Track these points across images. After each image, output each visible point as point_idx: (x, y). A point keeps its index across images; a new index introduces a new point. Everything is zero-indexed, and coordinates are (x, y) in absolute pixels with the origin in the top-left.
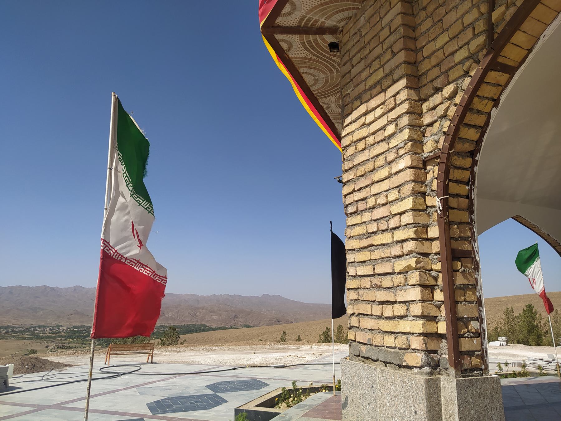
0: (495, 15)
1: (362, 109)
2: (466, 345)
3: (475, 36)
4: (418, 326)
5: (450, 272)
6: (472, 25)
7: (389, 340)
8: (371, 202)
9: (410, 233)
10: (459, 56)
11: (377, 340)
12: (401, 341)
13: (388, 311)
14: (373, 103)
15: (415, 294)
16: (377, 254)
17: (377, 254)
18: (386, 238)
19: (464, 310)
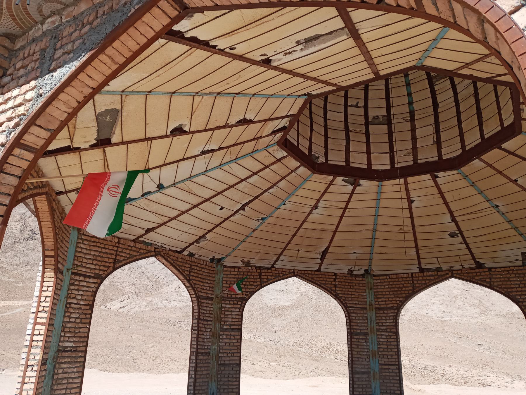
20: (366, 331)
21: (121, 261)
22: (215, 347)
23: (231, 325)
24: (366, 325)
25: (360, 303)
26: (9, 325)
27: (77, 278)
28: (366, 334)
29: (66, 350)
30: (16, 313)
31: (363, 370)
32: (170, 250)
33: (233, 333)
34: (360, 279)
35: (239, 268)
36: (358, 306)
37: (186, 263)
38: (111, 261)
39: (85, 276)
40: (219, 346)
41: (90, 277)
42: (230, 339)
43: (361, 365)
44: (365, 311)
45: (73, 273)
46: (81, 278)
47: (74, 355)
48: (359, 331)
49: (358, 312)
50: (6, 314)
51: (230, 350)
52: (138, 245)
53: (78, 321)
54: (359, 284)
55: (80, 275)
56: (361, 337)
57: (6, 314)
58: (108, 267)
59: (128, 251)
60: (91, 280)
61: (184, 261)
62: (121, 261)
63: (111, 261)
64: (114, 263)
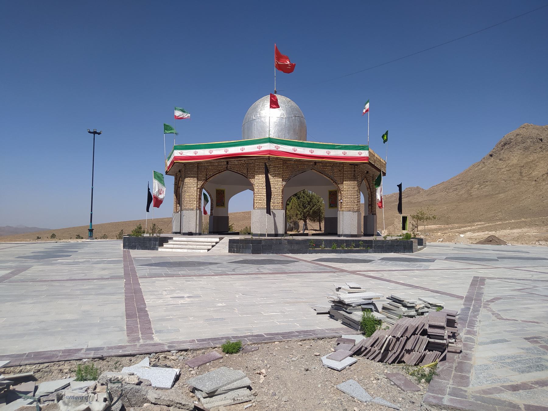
1: (190, 179)
2: (200, 208)
4: (196, 206)
5: (199, 201)
7: (192, 208)
8: (190, 191)
9: (196, 196)
10: (203, 178)
11: (190, 208)
12: (193, 208)
13: (192, 204)
14: (191, 179)
15: (196, 203)
16: (190, 198)
17: (190, 198)
18: (192, 196)
19: (200, 204)
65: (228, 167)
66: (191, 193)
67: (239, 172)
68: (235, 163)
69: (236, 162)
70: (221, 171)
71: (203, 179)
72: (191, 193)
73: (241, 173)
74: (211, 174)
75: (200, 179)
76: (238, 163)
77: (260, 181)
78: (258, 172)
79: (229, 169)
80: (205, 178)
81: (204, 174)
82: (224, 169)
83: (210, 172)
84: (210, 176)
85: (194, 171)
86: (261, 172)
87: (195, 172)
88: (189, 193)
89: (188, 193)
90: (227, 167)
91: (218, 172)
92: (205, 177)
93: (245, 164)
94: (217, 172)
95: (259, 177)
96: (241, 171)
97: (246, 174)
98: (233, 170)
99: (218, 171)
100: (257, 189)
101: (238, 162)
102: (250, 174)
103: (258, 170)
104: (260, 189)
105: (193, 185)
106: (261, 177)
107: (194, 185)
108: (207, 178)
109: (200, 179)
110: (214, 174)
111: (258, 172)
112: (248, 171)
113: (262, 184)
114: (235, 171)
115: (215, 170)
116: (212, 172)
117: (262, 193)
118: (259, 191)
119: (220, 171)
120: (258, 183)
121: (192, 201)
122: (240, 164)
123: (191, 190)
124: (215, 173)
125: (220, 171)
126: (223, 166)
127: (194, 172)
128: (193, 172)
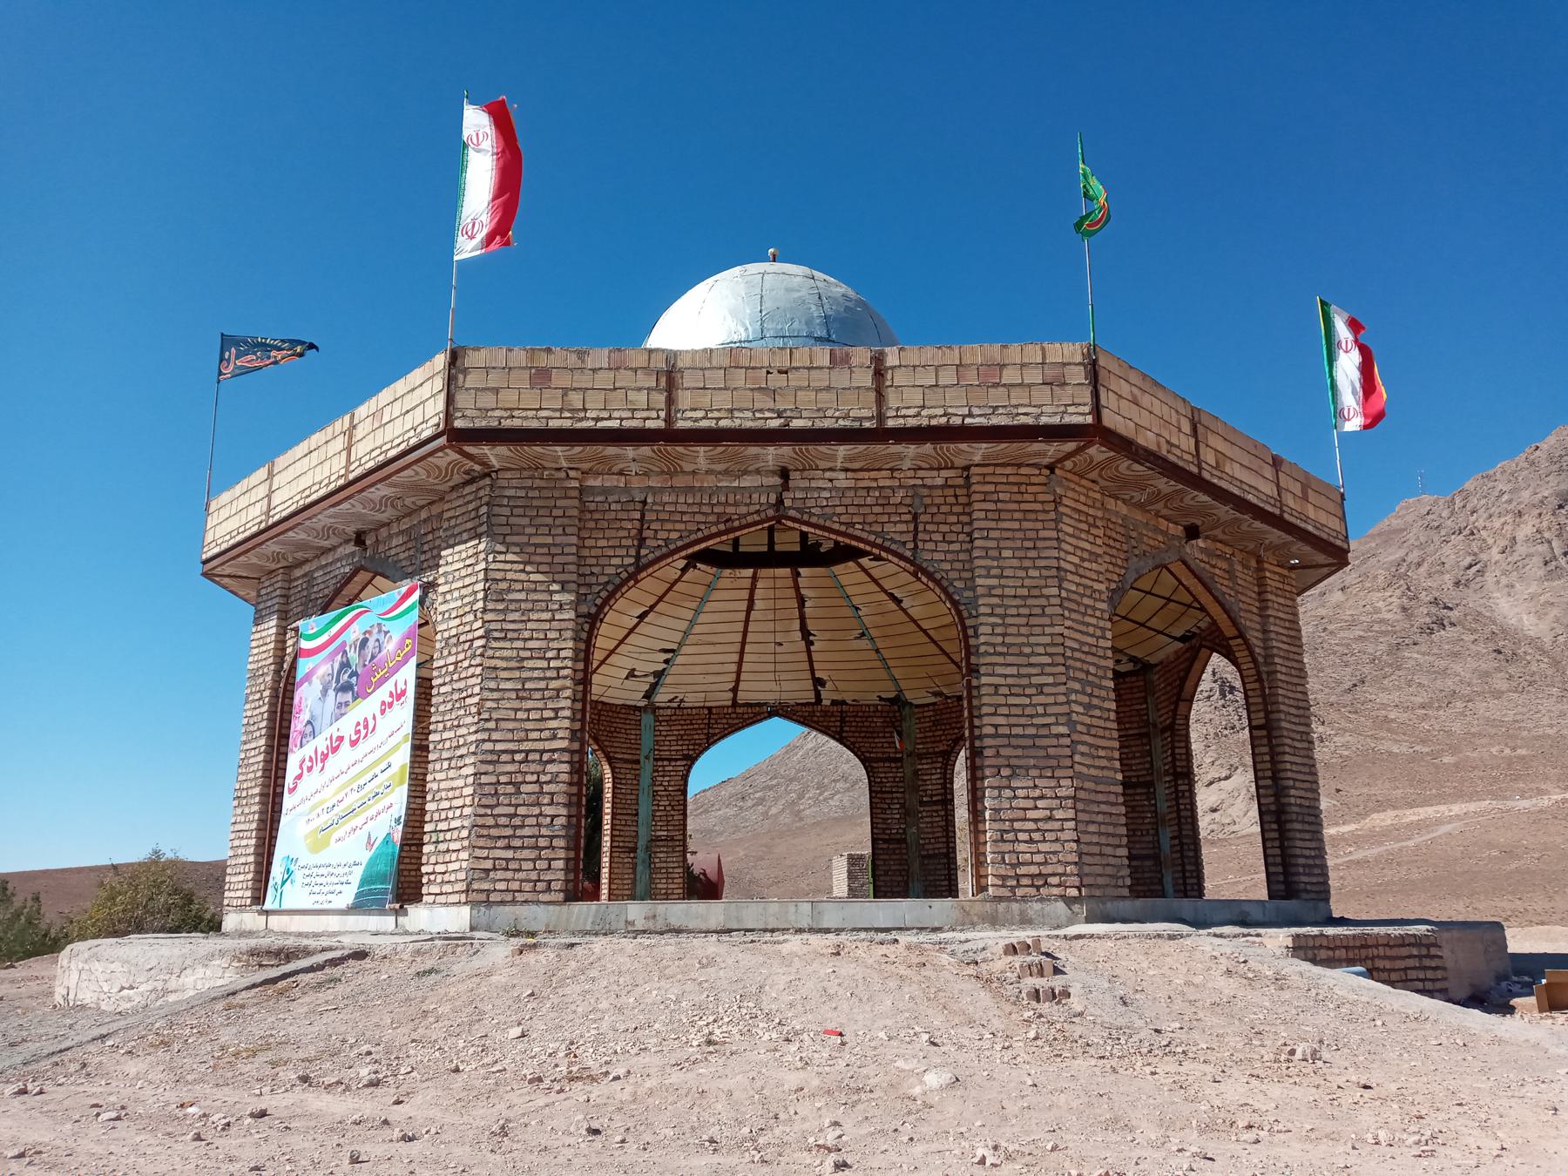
0: (643, 552)
3: (628, 555)
6: (628, 547)
8: (527, 634)
20: (1148, 778)
21: (715, 734)
22: (914, 830)
23: (931, 796)
24: (1147, 766)
25: (1135, 725)
26: (1416, 870)
27: (660, 763)
28: (1149, 784)
29: (658, 839)
30: (1440, 837)
31: (1145, 852)
32: (798, 704)
33: (935, 808)
34: (1134, 679)
35: (935, 704)
36: (1131, 732)
37: (833, 716)
38: (702, 736)
39: (669, 760)
40: (918, 828)
41: (676, 760)
42: (932, 816)
43: (1141, 842)
44: (1145, 741)
45: (655, 760)
46: (666, 763)
47: (670, 844)
48: (1134, 780)
49: (1132, 743)
50: (1411, 843)
51: (933, 833)
52: (739, 710)
53: (668, 808)
54: (1131, 688)
55: (663, 760)
56: (1139, 791)
57: (1411, 843)
58: (700, 745)
59: (724, 721)
60: (679, 763)
61: (826, 713)
62: (715, 734)
63: (702, 736)
64: (708, 739)
65: (788, 503)
66: (531, 644)
67: (858, 533)
68: (831, 480)
69: (842, 475)
70: (736, 524)
71: (617, 566)
72: (531, 644)
73: (872, 538)
74: (674, 535)
75: (594, 561)
76: (851, 483)
77: (1011, 582)
78: (993, 534)
79: (792, 513)
80: (632, 560)
81: (625, 533)
82: (757, 512)
83: (669, 526)
84: (664, 550)
85: (556, 512)
86: (1009, 534)
87: (566, 521)
88: (519, 644)
89: (507, 644)
90: (780, 501)
91: (722, 527)
92: (633, 552)
93: (901, 493)
94: (714, 530)
95: (1002, 563)
96: (878, 528)
97: (911, 545)
98: (821, 522)
99: (718, 523)
100: (994, 625)
101: (850, 475)
102: (930, 546)
103: (993, 524)
104: (1013, 630)
105: (545, 596)
106: (1015, 563)
107: (556, 597)
108: (644, 561)
109: (594, 561)
110: (693, 537)
111: (993, 534)
112: (921, 528)
113: (1018, 602)
114: (836, 526)
115: (699, 518)
116: (681, 526)
117: (1027, 650)
118: (1008, 640)
119: (729, 520)
120: (998, 592)
121: (538, 695)
122: (868, 489)
123: (530, 626)
124: (700, 535)
125: (729, 520)
126: (756, 496)
127: (558, 522)
128: (549, 521)
